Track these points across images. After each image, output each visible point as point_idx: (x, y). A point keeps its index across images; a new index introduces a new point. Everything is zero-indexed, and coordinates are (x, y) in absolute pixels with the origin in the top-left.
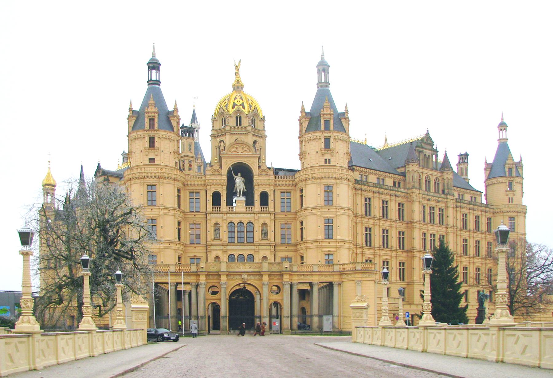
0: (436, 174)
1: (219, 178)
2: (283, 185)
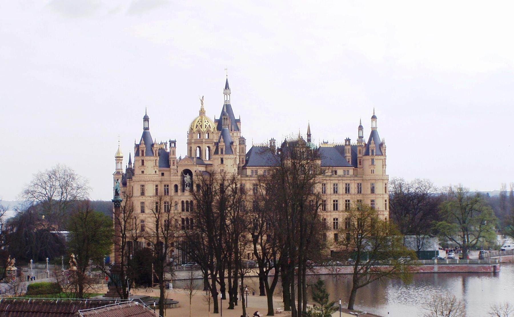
1: (177, 177)
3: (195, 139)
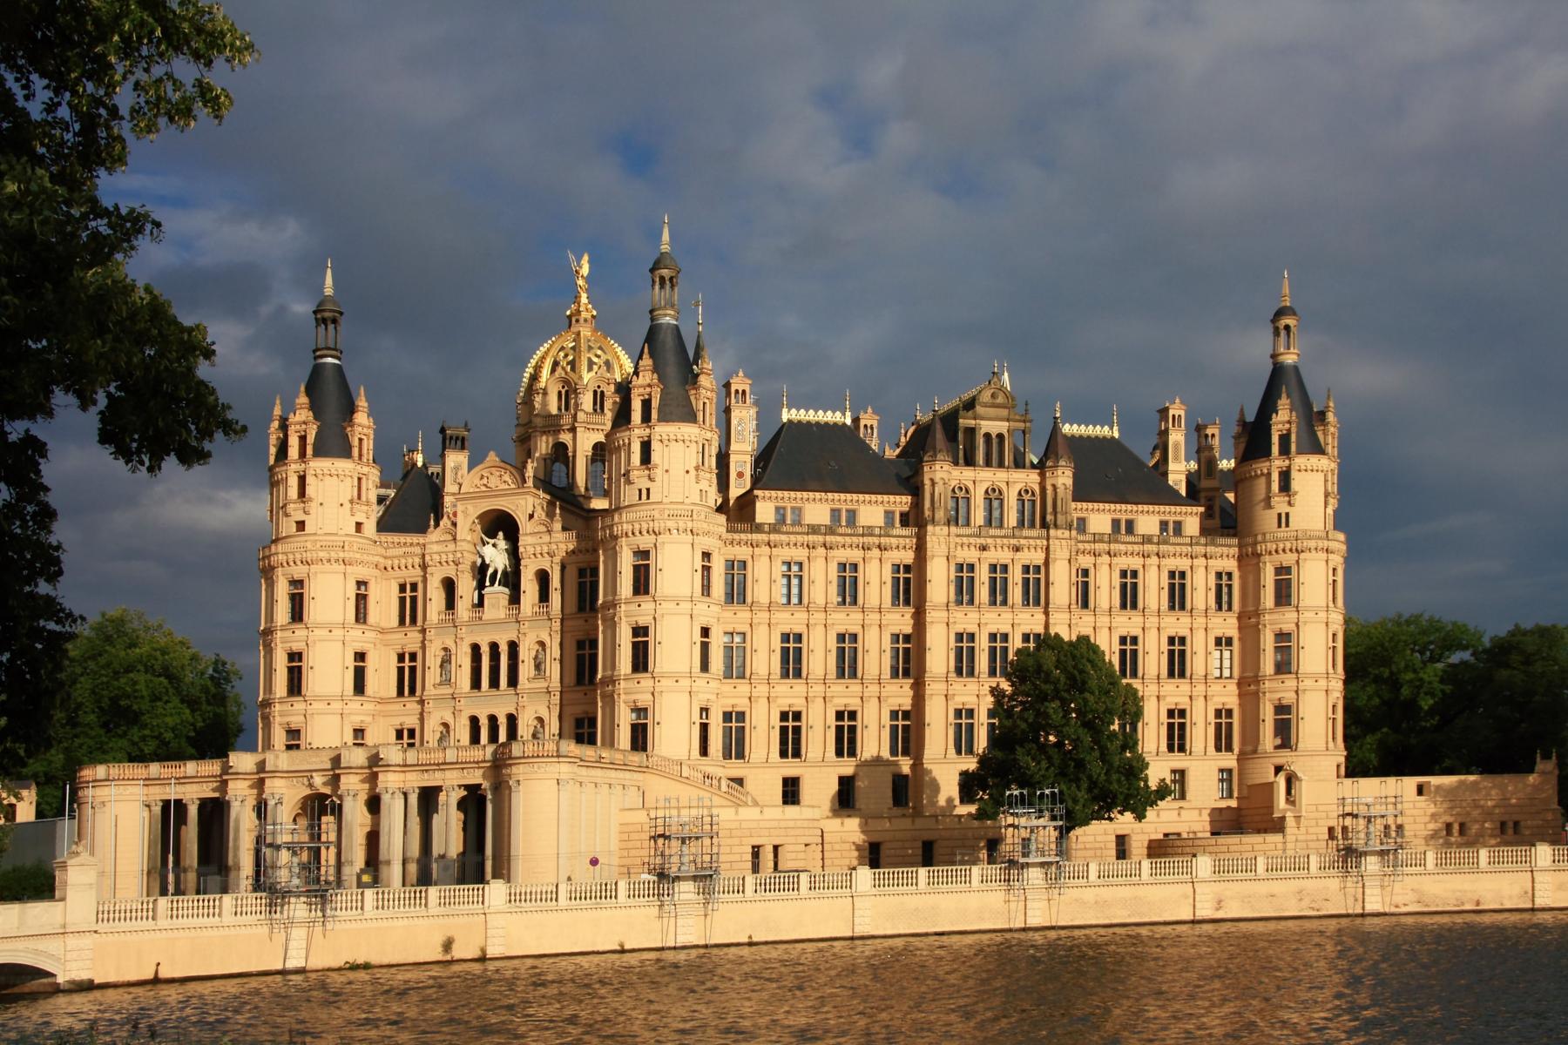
1: (451, 547)
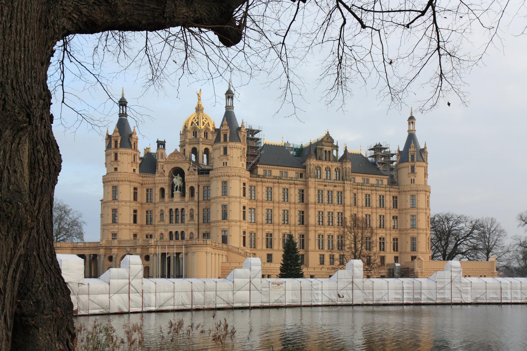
0: (337, 165)
1: (163, 178)
2: (204, 181)
3: (189, 139)
